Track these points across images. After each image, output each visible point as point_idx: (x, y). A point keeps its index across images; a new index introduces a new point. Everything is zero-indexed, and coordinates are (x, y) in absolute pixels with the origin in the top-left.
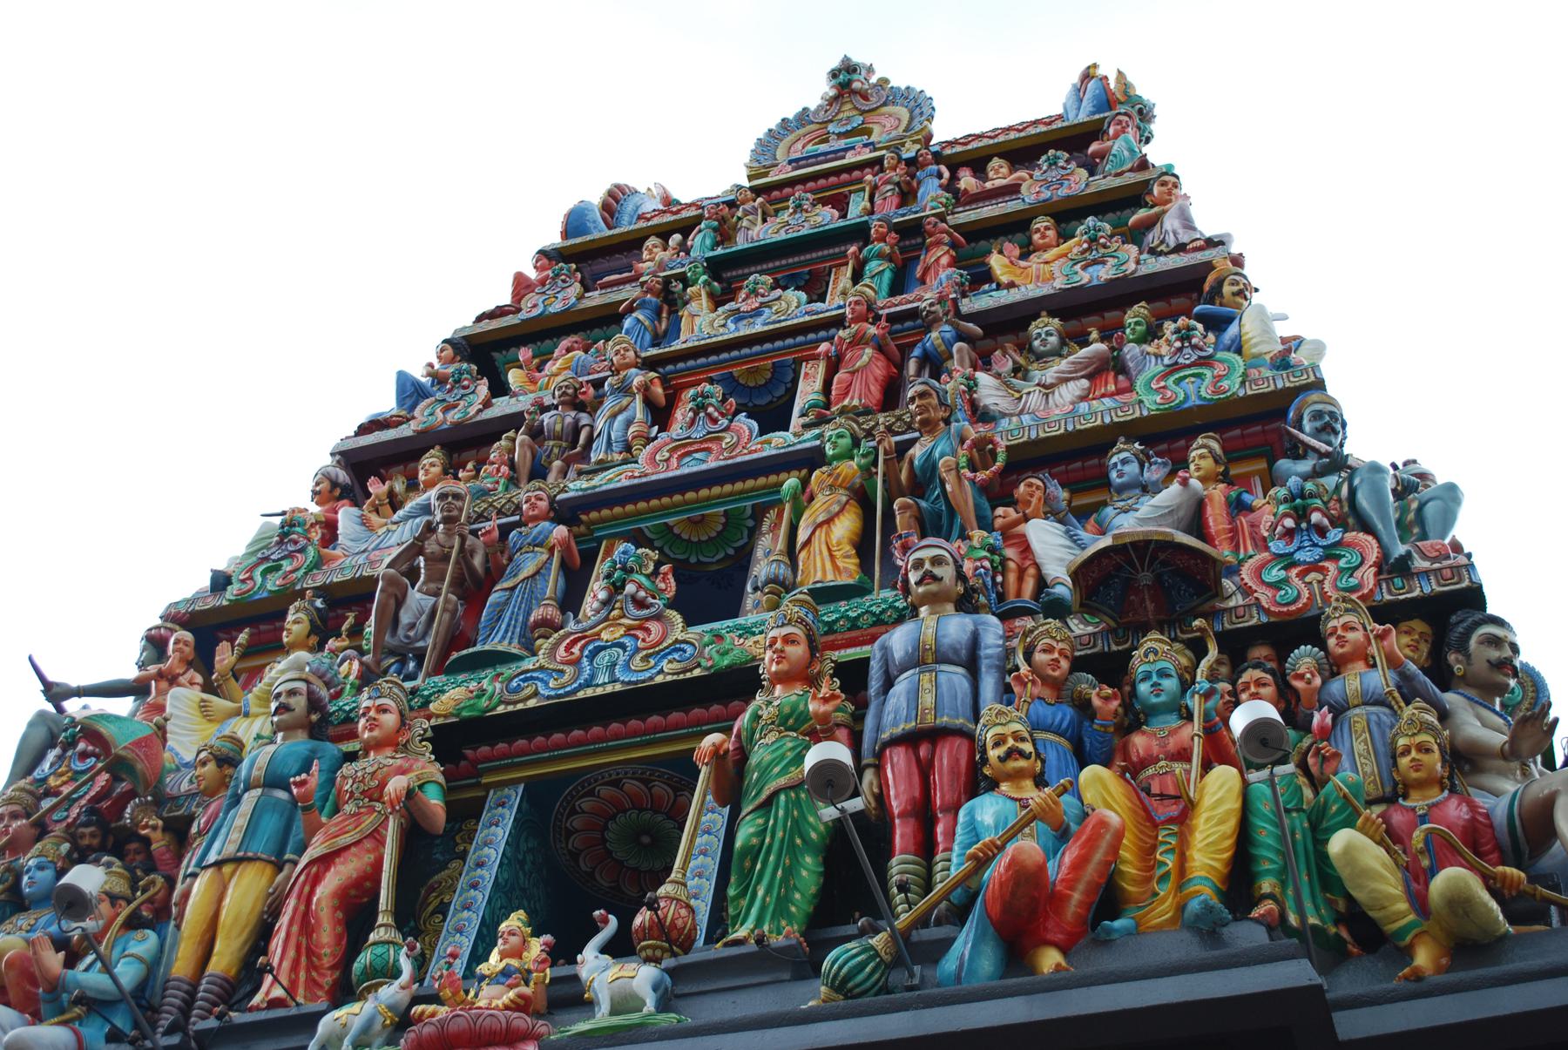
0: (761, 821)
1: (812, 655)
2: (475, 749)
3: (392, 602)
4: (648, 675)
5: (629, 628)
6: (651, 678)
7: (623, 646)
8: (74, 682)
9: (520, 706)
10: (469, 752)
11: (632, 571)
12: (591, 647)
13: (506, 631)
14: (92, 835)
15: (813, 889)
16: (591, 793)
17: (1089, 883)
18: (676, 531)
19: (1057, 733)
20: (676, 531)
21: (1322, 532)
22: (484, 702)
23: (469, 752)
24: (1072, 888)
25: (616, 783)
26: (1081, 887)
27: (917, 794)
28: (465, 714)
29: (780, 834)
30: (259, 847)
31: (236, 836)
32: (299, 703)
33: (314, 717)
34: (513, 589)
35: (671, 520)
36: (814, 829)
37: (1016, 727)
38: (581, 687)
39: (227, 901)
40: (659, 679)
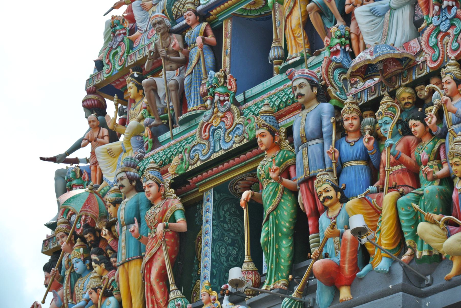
0: (267, 228)
1: (274, 136)
2: (192, 179)
3: (152, 93)
4: (230, 144)
5: (222, 118)
6: (232, 146)
7: (220, 127)
8: (63, 152)
9: (195, 166)
10: (190, 181)
11: (215, 87)
12: (211, 130)
13: (194, 98)
14: (90, 236)
15: (288, 255)
16: (237, 184)
17: (349, 260)
18: (248, 8)
19: (357, 160)
20: (248, 8)
21: (449, 8)
22: (184, 166)
23: (190, 181)
24: (344, 264)
25: (243, 179)
26: (347, 262)
27: (312, 206)
28: (180, 173)
29: (272, 236)
30: (132, 254)
31: (124, 251)
32: (125, 182)
33: (134, 184)
34: (191, 73)
35: (243, 6)
36: (285, 227)
37: (325, 186)
38: (212, 154)
39: (131, 278)
40: (235, 146)
